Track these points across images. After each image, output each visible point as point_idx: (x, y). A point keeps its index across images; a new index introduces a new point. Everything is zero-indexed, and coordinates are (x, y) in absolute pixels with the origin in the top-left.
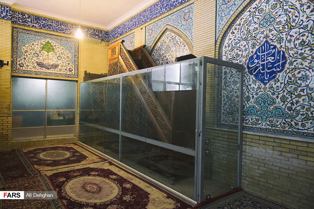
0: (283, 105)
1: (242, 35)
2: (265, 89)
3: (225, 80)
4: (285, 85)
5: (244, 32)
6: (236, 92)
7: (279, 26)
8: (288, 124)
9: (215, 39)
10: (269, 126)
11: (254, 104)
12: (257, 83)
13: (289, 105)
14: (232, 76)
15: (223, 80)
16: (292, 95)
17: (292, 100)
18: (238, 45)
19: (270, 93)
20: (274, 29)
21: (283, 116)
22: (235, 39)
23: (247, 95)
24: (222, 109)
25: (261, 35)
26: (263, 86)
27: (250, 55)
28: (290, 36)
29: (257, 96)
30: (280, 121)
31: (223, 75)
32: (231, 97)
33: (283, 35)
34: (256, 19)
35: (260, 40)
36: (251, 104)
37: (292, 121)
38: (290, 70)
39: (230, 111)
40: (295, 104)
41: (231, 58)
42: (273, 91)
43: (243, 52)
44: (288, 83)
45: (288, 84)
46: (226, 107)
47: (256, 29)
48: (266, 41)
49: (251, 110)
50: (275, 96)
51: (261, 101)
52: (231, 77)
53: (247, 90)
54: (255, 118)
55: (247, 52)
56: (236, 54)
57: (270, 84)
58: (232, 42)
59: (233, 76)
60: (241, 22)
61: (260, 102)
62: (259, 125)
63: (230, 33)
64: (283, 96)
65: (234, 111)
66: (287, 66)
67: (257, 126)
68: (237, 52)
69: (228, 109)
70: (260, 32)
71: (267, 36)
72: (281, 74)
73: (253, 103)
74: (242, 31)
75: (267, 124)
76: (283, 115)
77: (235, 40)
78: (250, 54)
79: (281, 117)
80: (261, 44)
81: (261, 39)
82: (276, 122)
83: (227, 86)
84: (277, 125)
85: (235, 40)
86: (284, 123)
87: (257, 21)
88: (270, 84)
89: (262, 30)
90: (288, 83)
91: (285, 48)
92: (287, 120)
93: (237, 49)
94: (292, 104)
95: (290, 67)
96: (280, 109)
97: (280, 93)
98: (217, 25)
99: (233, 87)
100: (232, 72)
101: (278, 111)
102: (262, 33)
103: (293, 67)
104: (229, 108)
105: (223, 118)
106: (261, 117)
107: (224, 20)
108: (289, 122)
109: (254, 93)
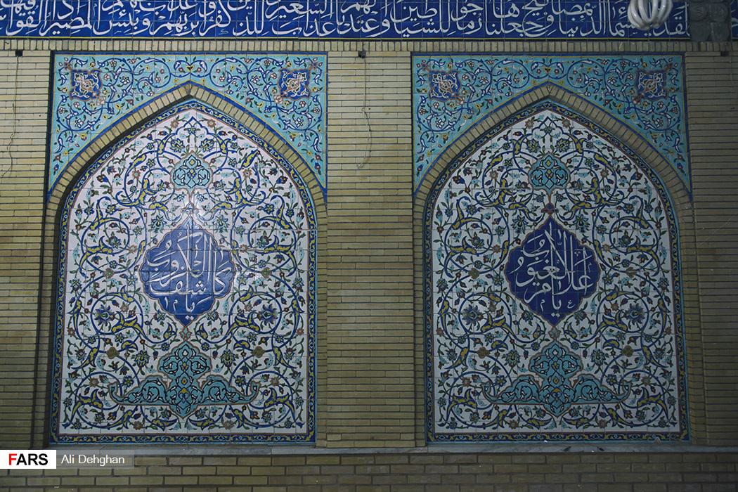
0: (226, 373)
1: (128, 191)
2: (555, 335)
3: (76, 306)
4: (230, 326)
5: (135, 184)
6: (477, 341)
7: (576, 192)
8: (237, 417)
9: (46, 183)
10: (196, 425)
11: (528, 373)
12: (535, 318)
13: (239, 372)
14: (96, 297)
15: (67, 305)
16: (615, 349)
17: (614, 360)
18: (116, 215)
19: (199, 346)
20: (565, 196)
21: (226, 398)
22: (108, 195)
23: (509, 350)
24: (437, 389)
25: (537, 204)
26: (549, 327)
27: (511, 248)
28: (601, 218)
29: (535, 353)
30: (220, 412)
31: (436, 289)
32: (463, 354)
33: (587, 214)
34: (164, 162)
35: (536, 215)
36: (523, 373)
37: (617, 407)
38: (608, 293)
39: (89, 395)
40: (621, 370)
41: (95, 247)
42: (206, 339)
43: (491, 234)
44: (236, 322)
45: (235, 325)
46: (448, 384)
47: (165, 186)
48: (550, 219)
49: (150, 388)
50: (209, 353)
51: (546, 364)
52: (95, 300)
53: (508, 335)
54: (536, 408)
55: (504, 238)
56: (110, 239)
57: (197, 324)
58: (98, 204)
59: (99, 297)
60: (127, 156)
61: (545, 367)
62: (545, 427)
63: (94, 177)
64: (227, 353)
65: (103, 394)
66: (600, 283)
67: (542, 429)
68: (113, 233)
69: (456, 389)
70: (175, 196)
71: (550, 208)
72: (589, 300)
73: (155, 371)
74: (128, 179)
75: (565, 419)
76: (600, 396)
77: (107, 198)
78: (149, 244)
79: (595, 399)
80: (539, 225)
81: (178, 212)
82: (585, 413)
83: (81, 323)
84: (214, 422)
85: (107, 198)
86: (602, 414)
87: (526, 167)
88: (197, 324)
89: (539, 193)
90: (238, 324)
91: (231, 244)
92: (607, 406)
93: (475, 226)
94: (616, 368)
95: (608, 287)
96: (592, 380)
97: (588, 343)
98: (54, 148)
99: (99, 328)
100: (463, 285)
101: (587, 386)
102: (540, 199)
103: (611, 287)
104: (458, 386)
105: (67, 416)
106: (551, 404)
107: (77, 140)
108: (239, 411)
109: (529, 345)
